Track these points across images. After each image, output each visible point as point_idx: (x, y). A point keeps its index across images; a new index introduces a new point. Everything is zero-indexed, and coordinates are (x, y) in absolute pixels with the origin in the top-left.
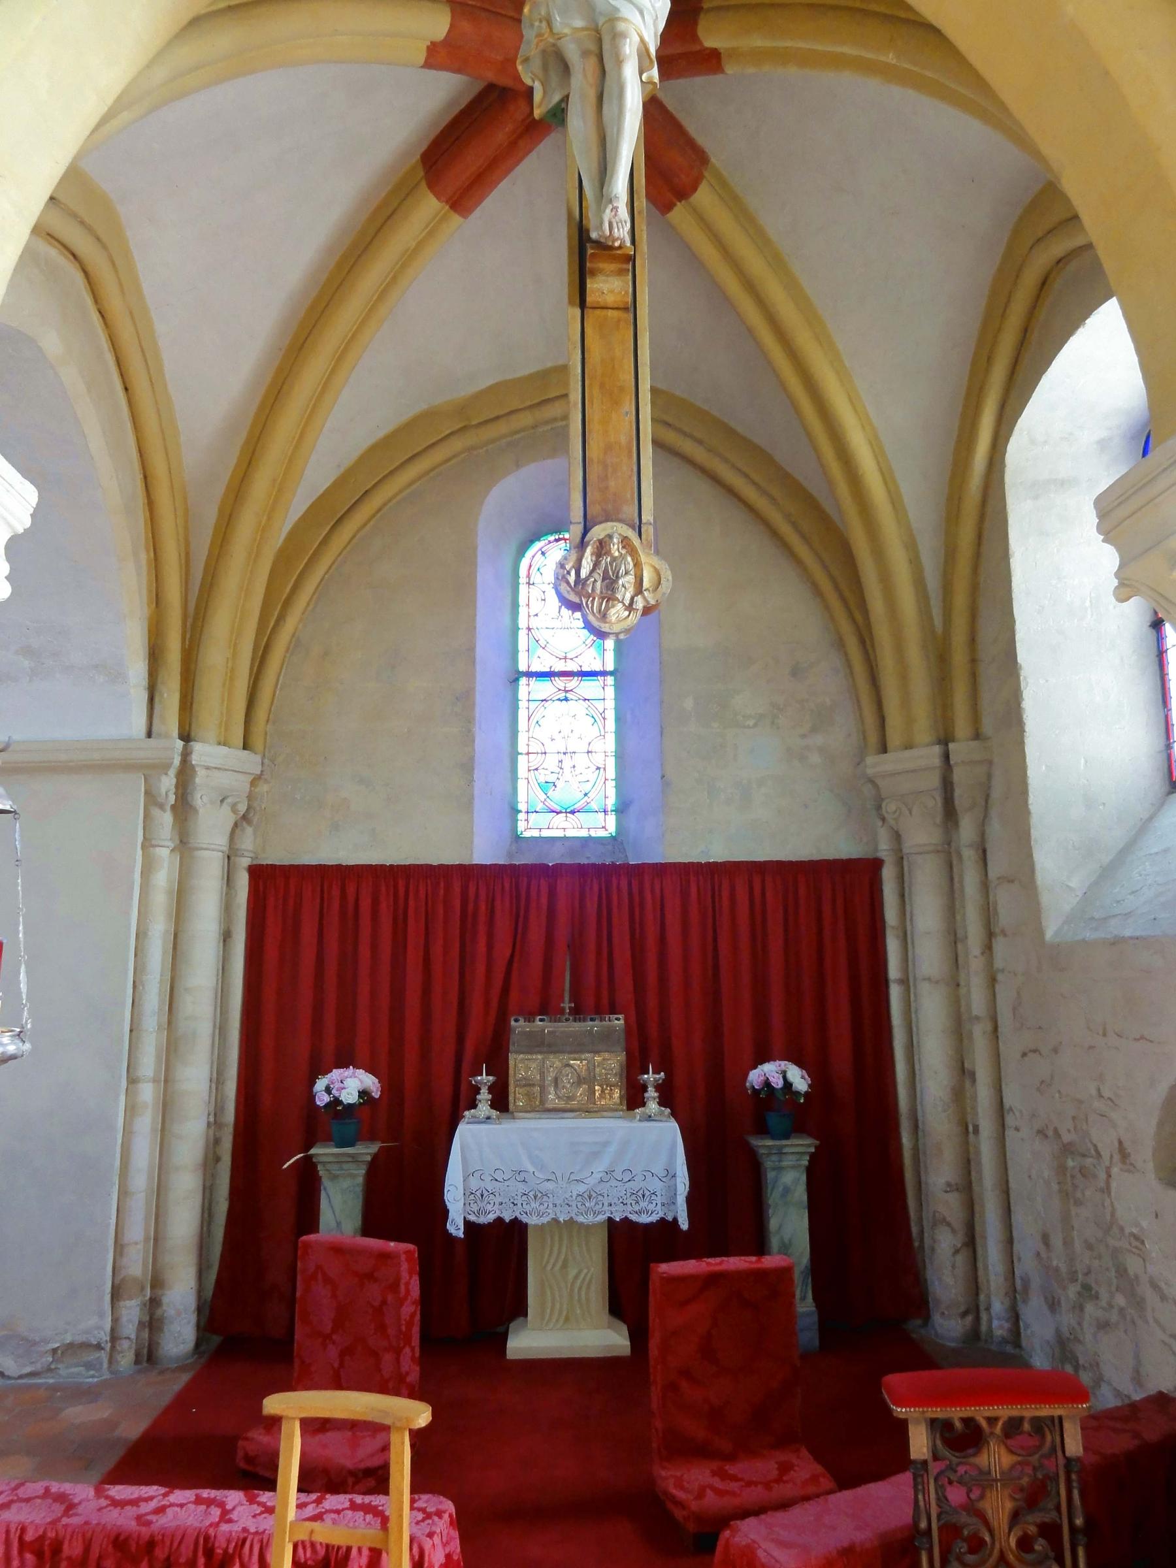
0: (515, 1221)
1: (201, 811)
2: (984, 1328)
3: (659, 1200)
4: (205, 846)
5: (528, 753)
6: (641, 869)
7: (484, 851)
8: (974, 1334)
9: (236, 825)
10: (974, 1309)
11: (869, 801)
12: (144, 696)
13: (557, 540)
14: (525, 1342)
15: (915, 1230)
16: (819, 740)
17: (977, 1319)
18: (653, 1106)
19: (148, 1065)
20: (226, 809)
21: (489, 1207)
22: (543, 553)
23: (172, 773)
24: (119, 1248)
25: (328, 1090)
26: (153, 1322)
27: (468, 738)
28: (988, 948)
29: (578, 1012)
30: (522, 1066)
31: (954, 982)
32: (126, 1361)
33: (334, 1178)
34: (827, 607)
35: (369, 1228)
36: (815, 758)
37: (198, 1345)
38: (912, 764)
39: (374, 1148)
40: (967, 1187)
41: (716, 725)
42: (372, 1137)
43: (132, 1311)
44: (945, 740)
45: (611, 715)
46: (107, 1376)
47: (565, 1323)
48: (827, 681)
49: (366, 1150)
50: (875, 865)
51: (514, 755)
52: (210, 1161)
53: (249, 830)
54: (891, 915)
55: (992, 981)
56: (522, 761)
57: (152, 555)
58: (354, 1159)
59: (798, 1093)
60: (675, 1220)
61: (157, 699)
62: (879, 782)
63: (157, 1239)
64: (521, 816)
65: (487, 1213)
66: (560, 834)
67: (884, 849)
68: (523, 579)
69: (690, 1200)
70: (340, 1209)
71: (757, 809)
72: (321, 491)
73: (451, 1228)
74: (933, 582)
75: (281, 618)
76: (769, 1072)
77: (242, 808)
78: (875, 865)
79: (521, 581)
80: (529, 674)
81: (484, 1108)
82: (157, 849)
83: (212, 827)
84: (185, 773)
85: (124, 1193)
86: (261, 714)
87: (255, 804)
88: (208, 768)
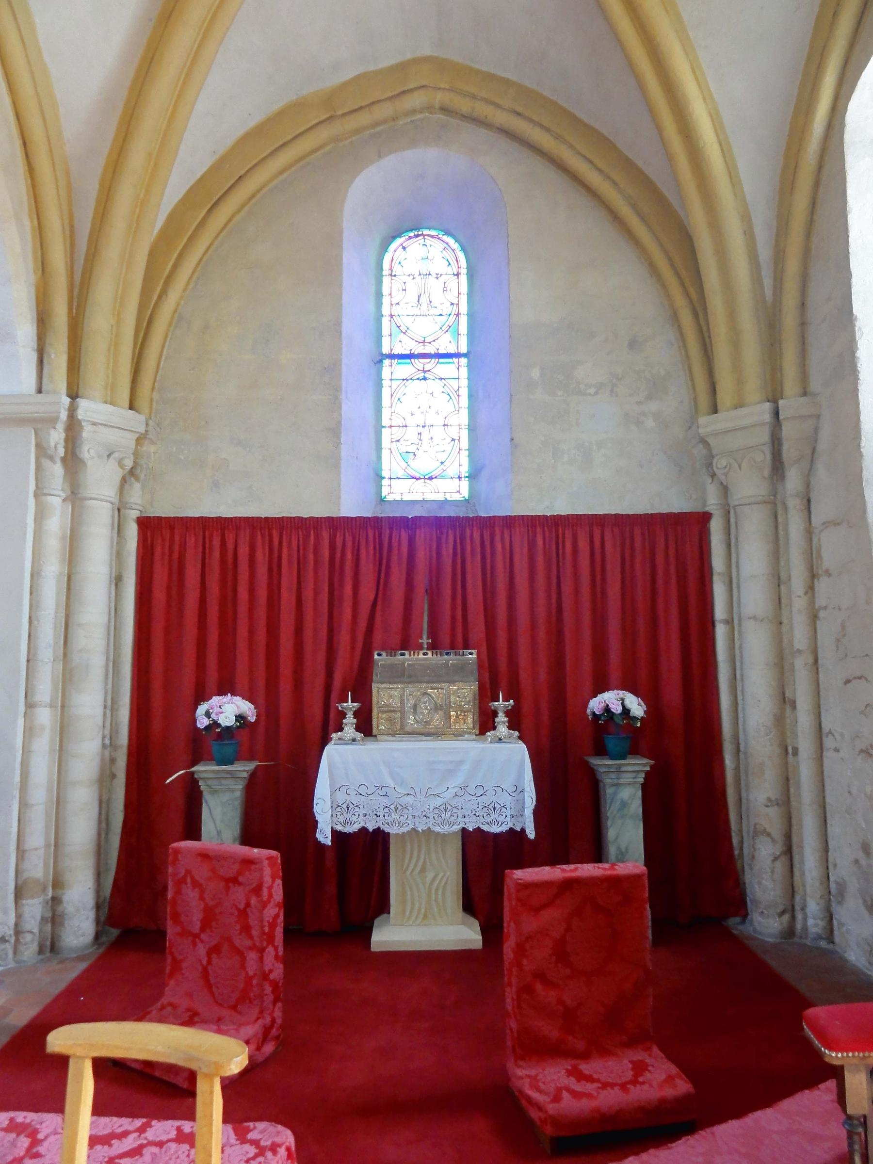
0: (378, 831)
1: (89, 463)
2: (799, 926)
3: (509, 812)
4: (93, 496)
5: (391, 426)
7: (351, 505)
8: (790, 932)
9: (124, 480)
10: (790, 907)
11: (701, 458)
12: (34, 356)
13: (416, 236)
14: (389, 935)
15: (735, 840)
16: (653, 406)
17: (793, 918)
18: (502, 729)
19: (45, 690)
20: (112, 464)
21: (354, 818)
22: (404, 248)
23: (61, 427)
24: (21, 853)
25: (208, 714)
26: (55, 917)
27: (335, 403)
28: (811, 589)
29: (434, 646)
30: (384, 695)
31: (778, 620)
32: (29, 951)
33: (214, 792)
34: (663, 286)
35: (248, 838)
36: (650, 423)
37: (97, 936)
38: (743, 422)
39: (251, 766)
40: (786, 803)
41: (560, 393)
42: (251, 758)
43: (34, 909)
44: (774, 398)
45: (464, 392)
46: (12, 965)
47: (423, 919)
48: (662, 353)
49: (244, 768)
50: (704, 518)
51: (379, 428)
52: (105, 779)
53: (137, 486)
54: (718, 562)
55: (814, 617)
56: (385, 432)
57: (36, 222)
58: (232, 775)
59: (635, 718)
60: (523, 831)
61: (45, 361)
62: (711, 441)
63: (57, 846)
64: (385, 482)
65: (352, 823)
66: (419, 497)
67: (712, 504)
68: (386, 271)
69: (537, 813)
70: (221, 819)
71: (598, 467)
72: (198, 176)
73: (320, 837)
74: (765, 253)
75: (164, 293)
76: (611, 699)
77: (129, 463)
78: (704, 518)
79: (384, 273)
80: (392, 356)
81: (349, 730)
82: (50, 498)
83: (102, 480)
84: (73, 427)
85: (24, 805)
87: (142, 462)
88: (94, 424)
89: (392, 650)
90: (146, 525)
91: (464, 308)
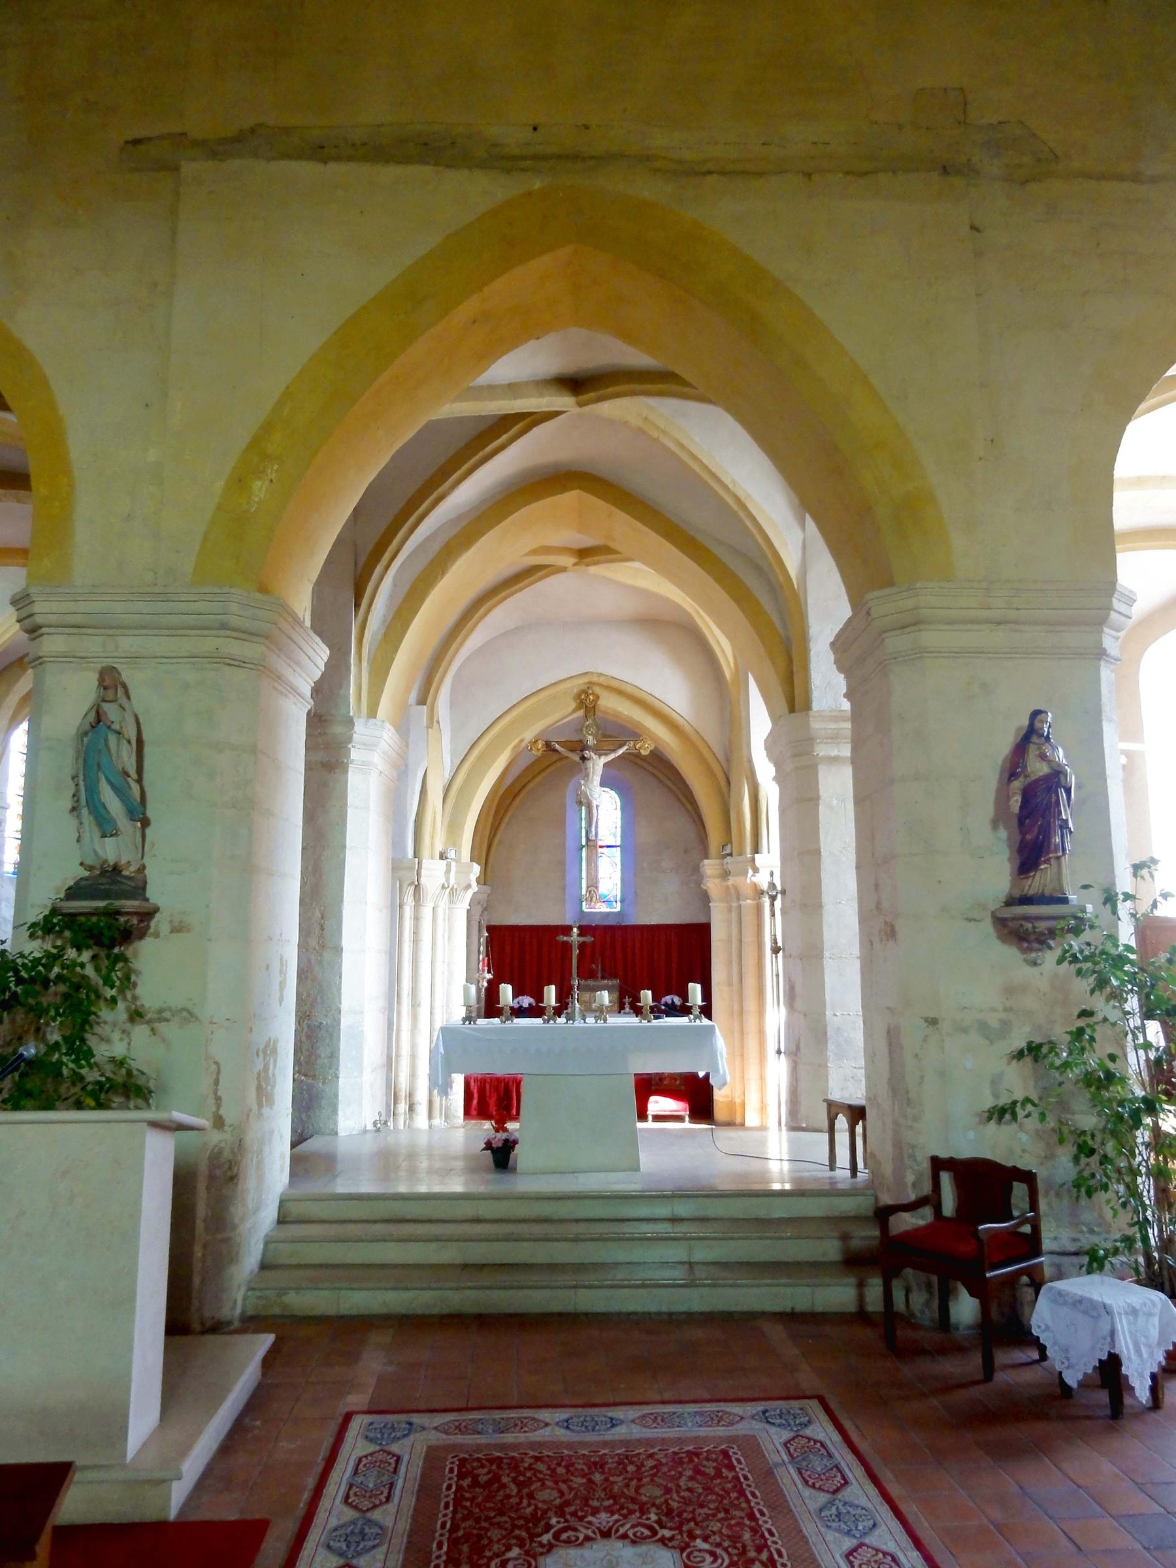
6: (626, 927)
18: (627, 1010)
27: (563, 877)
29: (603, 978)
75: (495, 834)
90: (490, 929)
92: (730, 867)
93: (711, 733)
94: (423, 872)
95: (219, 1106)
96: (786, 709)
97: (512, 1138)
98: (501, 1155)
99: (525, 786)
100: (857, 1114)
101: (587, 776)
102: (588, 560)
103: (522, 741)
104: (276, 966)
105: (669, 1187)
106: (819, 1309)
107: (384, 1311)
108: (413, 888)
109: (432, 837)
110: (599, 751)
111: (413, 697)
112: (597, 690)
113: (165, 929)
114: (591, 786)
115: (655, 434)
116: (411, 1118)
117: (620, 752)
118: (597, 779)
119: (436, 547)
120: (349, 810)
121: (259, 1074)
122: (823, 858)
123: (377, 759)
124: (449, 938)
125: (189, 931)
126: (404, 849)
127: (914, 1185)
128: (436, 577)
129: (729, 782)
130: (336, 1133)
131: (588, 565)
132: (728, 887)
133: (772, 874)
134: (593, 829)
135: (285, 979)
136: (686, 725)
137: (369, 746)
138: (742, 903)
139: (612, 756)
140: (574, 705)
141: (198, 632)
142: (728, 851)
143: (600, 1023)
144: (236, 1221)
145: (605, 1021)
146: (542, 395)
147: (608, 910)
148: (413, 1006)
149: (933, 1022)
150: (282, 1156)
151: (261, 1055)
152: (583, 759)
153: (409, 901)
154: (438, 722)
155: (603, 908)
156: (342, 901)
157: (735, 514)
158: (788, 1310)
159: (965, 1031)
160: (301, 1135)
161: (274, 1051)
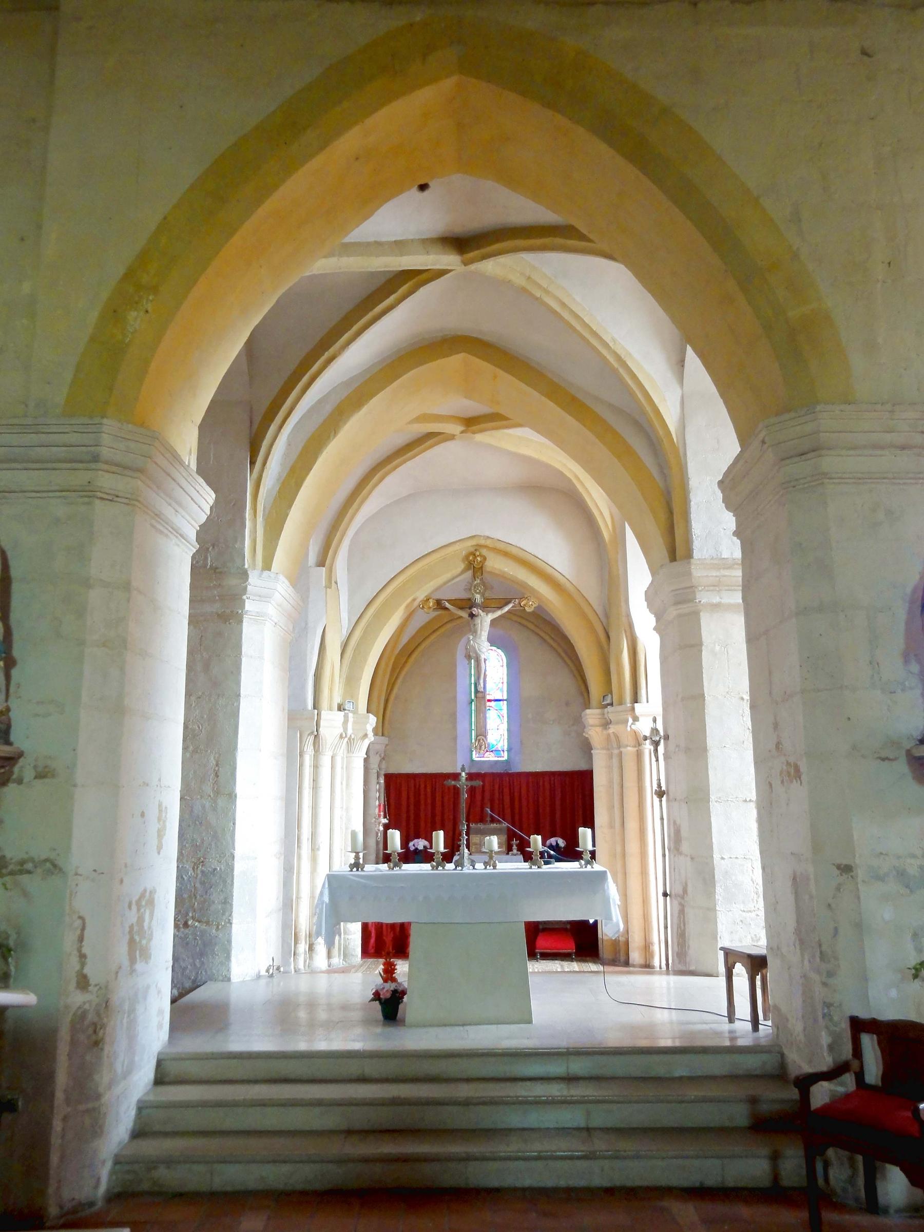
18: (515, 851)
75: (392, 690)
86: (386, 722)
89: (476, 822)
91: (505, 680)
92: (611, 717)
93: (591, 591)
94: (322, 723)
95: (83, 964)
96: (667, 560)
97: (400, 989)
98: (390, 1005)
99: (419, 644)
100: (757, 964)
101: (475, 632)
102: (474, 428)
103: (414, 600)
104: (152, 814)
105: (562, 1043)
106: (731, 1184)
107: (261, 1187)
108: (312, 737)
109: (331, 690)
110: (486, 607)
111: (312, 558)
112: (484, 552)
113: (29, 774)
114: (478, 641)
115: (538, 294)
116: (311, 958)
117: (506, 609)
118: (484, 635)
119: (328, 408)
120: (244, 660)
121: (131, 927)
122: (707, 702)
123: (271, 610)
124: (347, 785)
125: (53, 776)
126: (305, 701)
127: (831, 1048)
128: (329, 437)
129: (608, 637)
130: (229, 980)
131: (474, 433)
132: (609, 735)
133: (655, 720)
134: (482, 681)
135: (164, 827)
136: (568, 585)
137: (264, 598)
138: (622, 749)
139: (499, 613)
140: (462, 566)
141: (69, 465)
142: (609, 701)
143: (490, 870)
144: (101, 1090)
145: (495, 867)
146: (428, 253)
147: (496, 759)
148: (313, 850)
149: (846, 869)
150: (161, 1012)
151: (134, 907)
152: (472, 616)
153: (309, 750)
154: (336, 583)
155: (490, 757)
156: (235, 748)
157: (615, 372)
158: (697, 1185)
159: (881, 878)
160: (194, 981)
161: (151, 903)
